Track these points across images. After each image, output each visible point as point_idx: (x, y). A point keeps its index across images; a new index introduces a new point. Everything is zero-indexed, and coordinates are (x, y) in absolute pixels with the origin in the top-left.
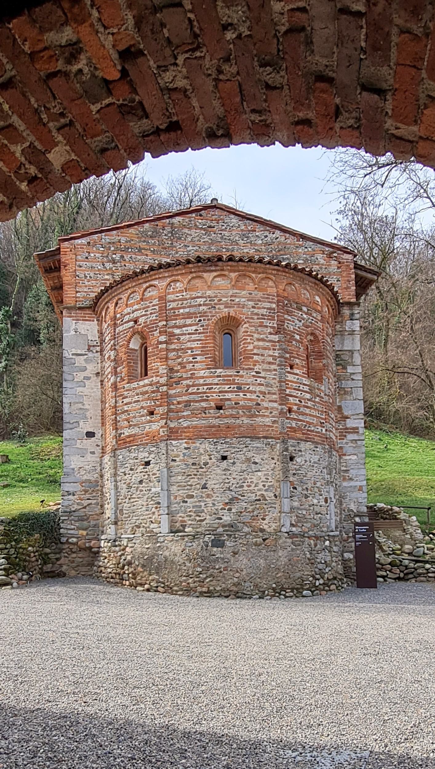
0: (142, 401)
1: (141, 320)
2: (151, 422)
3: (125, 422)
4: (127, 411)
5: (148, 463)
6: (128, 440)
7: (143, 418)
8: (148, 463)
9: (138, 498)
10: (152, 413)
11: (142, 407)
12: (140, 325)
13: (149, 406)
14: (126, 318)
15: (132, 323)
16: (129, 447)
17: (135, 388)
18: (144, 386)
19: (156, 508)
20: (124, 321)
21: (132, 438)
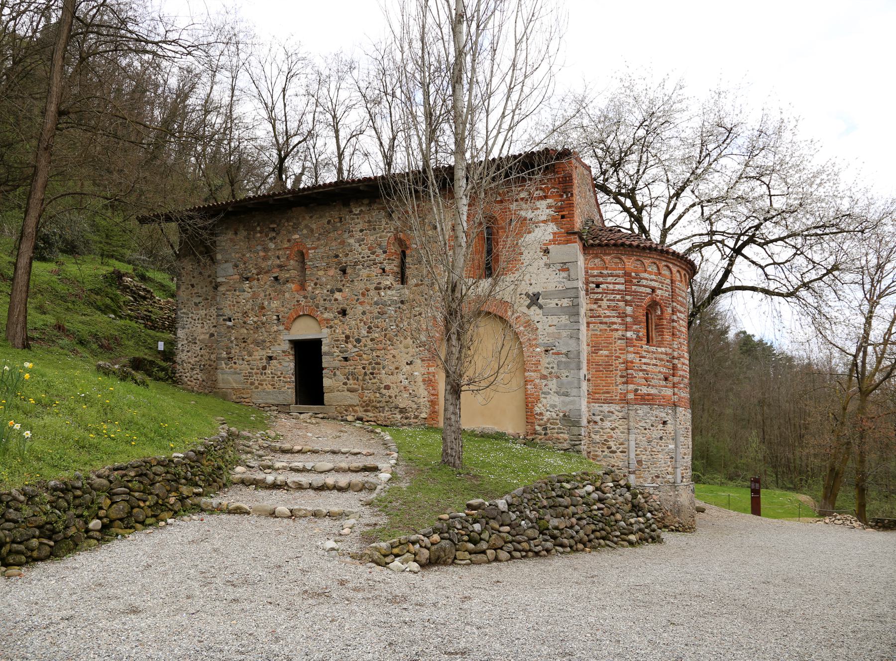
2: (666, 387)
4: (644, 370)
5: (665, 423)
8: (665, 423)
10: (666, 379)
11: (660, 372)
17: (653, 352)
18: (662, 353)
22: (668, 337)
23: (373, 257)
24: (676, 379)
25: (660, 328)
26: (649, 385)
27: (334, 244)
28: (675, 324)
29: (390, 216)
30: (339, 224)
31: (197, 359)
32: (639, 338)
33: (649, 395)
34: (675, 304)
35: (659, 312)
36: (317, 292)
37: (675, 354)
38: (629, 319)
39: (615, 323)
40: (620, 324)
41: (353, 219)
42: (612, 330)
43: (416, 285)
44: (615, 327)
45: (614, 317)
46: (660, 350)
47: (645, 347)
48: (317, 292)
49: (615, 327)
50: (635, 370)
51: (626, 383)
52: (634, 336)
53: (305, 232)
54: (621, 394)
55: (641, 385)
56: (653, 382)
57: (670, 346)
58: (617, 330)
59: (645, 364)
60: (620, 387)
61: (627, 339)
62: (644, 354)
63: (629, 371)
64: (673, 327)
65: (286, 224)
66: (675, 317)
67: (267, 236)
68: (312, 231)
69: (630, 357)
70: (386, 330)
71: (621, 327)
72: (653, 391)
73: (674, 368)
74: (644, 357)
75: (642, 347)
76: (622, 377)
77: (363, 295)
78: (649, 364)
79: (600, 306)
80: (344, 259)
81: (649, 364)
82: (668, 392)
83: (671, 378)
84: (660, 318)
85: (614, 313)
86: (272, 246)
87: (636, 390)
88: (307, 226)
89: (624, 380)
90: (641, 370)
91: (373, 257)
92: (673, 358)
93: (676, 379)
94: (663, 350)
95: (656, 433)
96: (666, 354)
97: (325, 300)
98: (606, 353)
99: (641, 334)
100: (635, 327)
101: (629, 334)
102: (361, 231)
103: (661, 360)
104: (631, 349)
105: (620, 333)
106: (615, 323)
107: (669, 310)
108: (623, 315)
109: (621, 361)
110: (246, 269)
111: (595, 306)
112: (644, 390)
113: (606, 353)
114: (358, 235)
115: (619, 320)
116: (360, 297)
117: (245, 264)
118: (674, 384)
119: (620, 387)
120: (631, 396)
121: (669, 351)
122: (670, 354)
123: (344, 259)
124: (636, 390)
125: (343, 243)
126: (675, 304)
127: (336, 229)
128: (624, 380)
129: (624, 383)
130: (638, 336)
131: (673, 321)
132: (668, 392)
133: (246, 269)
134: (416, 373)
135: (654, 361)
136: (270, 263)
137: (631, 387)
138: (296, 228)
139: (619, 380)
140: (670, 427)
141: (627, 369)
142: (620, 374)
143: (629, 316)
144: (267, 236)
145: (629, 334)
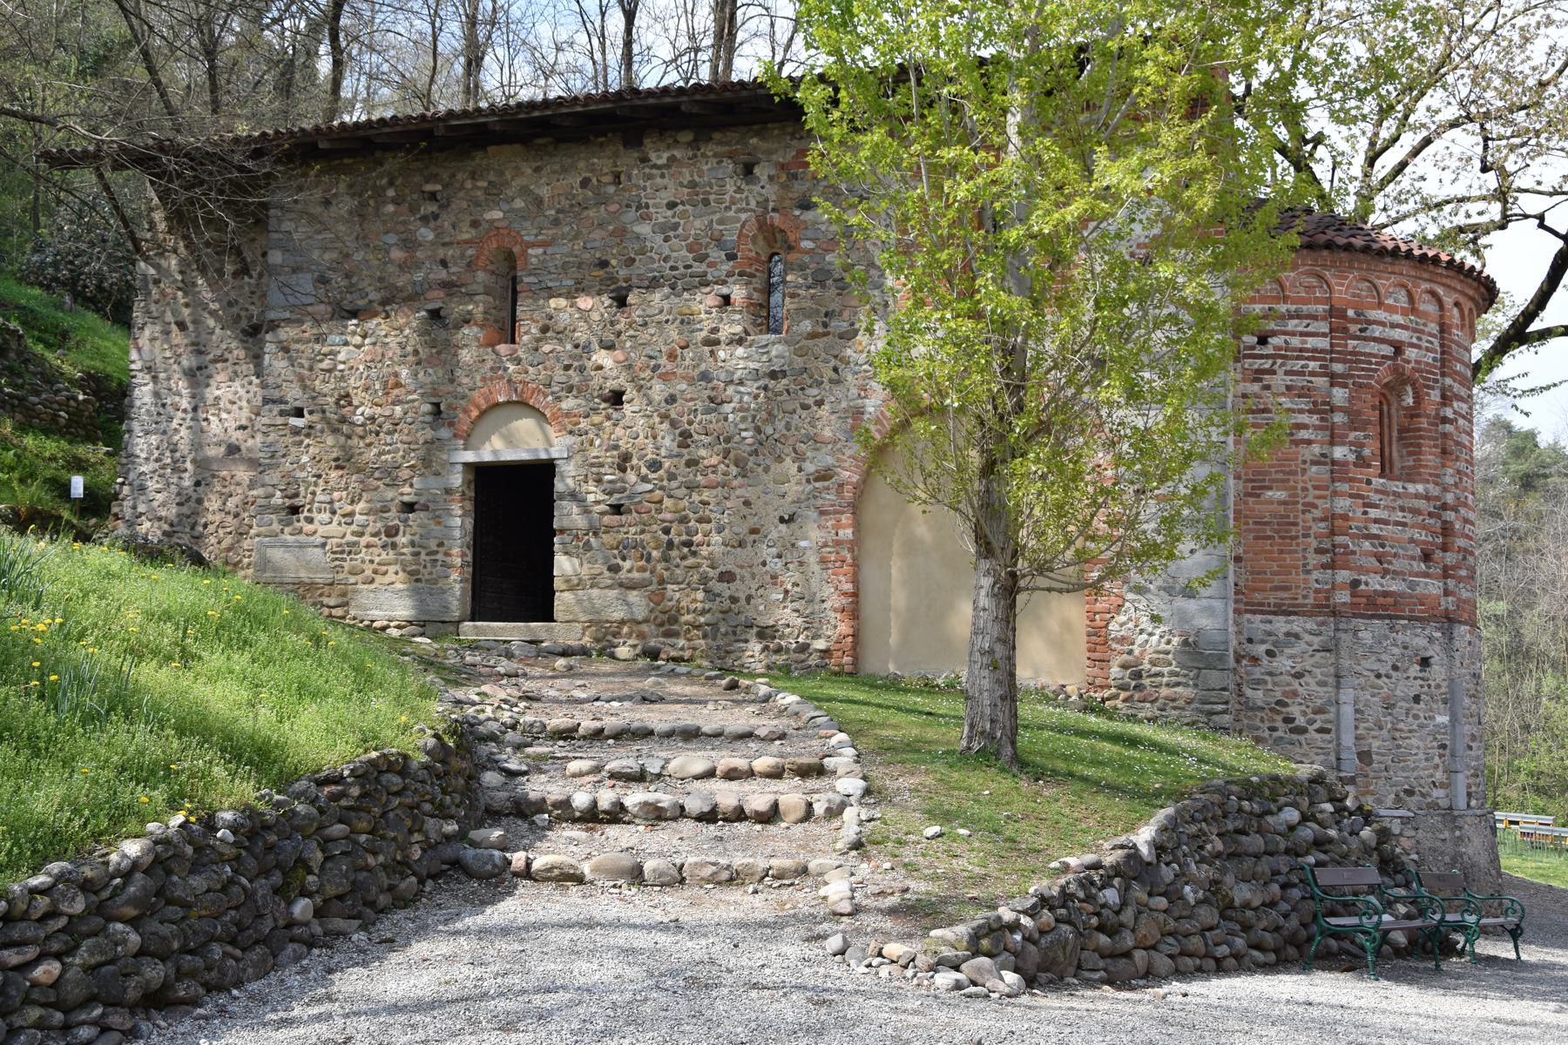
0: (1413, 527)
1: (1411, 353)
2: (1426, 575)
3: (1373, 560)
4: (1377, 537)
5: (1425, 662)
6: (1381, 600)
7: (1414, 563)
9: (1410, 731)
10: (1426, 557)
11: (1412, 540)
12: (1409, 362)
13: (1424, 542)
14: (1377, 331)
15: (1388, 350)
16: (1390, 617)
17: (1397, 495)
18: (1417, 496)
19: (1441, 756)
20: (1368, 334)
21: (1390, 600)
22: (1430, 458)
23: (699, 268)
24: (1450, 558)
25: (1409, 436)
26: (1386, 572)
27: (597, 234)
28: (1449, 428)
29: (748, 171)
30: (611, 189)
31: (185, 510)
32: (1362, 462)
33: (1386, 594)
34: (1448, 381)
35: (1410, 401)
36: (547, 348)
37: (1449, 498)
38: (1339, 418)
39: (1305, 427)
40: (1316, 428)
41: (650, 177)
42: (1297, 443)
43: (813, 336)
44: (1304, 434)
45: (1301, 411)
46: (1411, 488)
47: (1378, 482)
48: (547, 348)
49: (1304, 434)
50: (1352, 536)
51: (1331, 566)
52: (1352, 458)
53: (519, 203)
54: (1317, 591)
55: (1367, 572)
56: (1397, 565)
57: (1437, 478)
58: (1309, 442)
59: (1376, 521)
60: (1316, 575)
61: (1334, 462)
62: (1375, 498)
63: (1339, 539)
64: (1445, 435)
65: (469, 185)
66: (1449, 412)
67: (413, 209)
68: (539, 202)
69: (1342, 504)
70: (728, 440)
71: (1321, 436)
72: (1395, 586)
73: (1447, 529)
74: (1376, 506)
75: (1369, 482)
76: (1319, 551)
77: (672, 356)
78: (1386, 522)
79: (1267, 387)
80: (623, 273)
81: (1386, 522)
82: (1433, 587)
83: (1438, 554)
84: (1413, 413)
85: (1303, 403)
86: (426, 234)
87: (1355, 584)
88: (524, 191)
89: (1325, 559)
90: (1368, 537)
91: (699, 268)
92: (1445, 507)
93: (1450, 558)
94: (1420, 488)
95: (1405, 687)
96: (1427, 498)
97: (567, 368)
98: (1280, 495)
99: (1367, 452)
100: (1352, 435)
101: (1339, 452)
102: (671, 205)
103: (1415, 512)
104: (1345, 487)
105: (1316, 449)
106: (1305, 427)
107: (1435, 395)
108: (1324, 409)
109: (1317, 513)
110: (351, 288)
111: (1256, 387)
112: (1374, 583)
113: (1280, 495)
114: (662, 215)
115: (1314, 419)
116: (663, 361)
117: (348, 276)
118: (1446, 569)
119: (1316, 575)
120: (1343, 597)
121: (1434, 490)
122: (1437, 498)
123: (623, 273)
124: (1355, 584)
125: (621, 233)
126: (1448, 381)
127: (603, 201)
128: (1325, 559)
129: (1324, 567)
130: (1359, 457)
131: (1445, 420)
132: (1433, 587)
133: (351, 288)
134: (803, 544)
135: (1399, 516)
136: (419, 276)
137: (1344, 576)
138: (494, 194)
139: (1313, 559)
140: (1438, 672)
141: (1333, 533)
142: (1314, 544)
143: (1340, 409)
144: (413, 209)
145: (1339, 452)
